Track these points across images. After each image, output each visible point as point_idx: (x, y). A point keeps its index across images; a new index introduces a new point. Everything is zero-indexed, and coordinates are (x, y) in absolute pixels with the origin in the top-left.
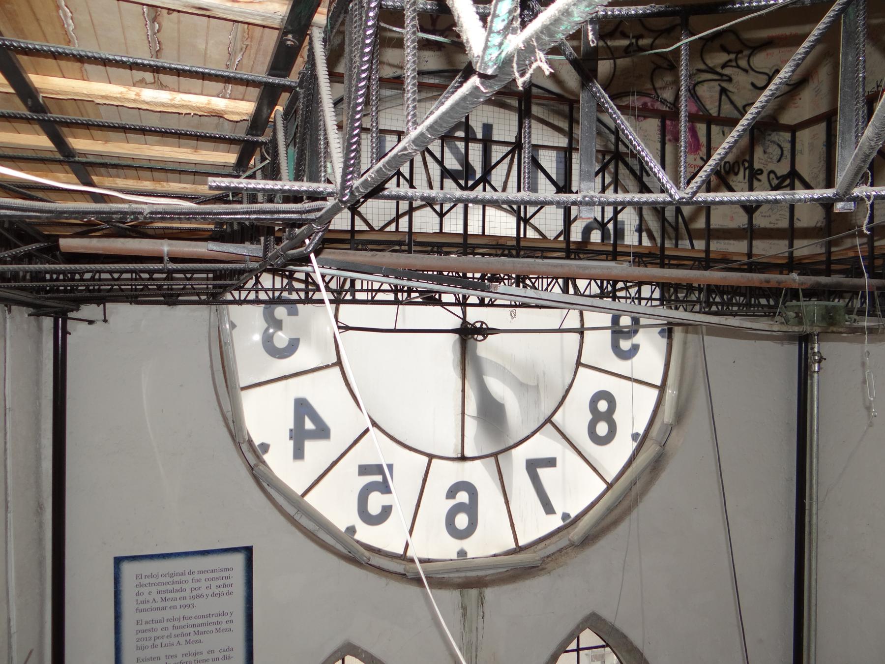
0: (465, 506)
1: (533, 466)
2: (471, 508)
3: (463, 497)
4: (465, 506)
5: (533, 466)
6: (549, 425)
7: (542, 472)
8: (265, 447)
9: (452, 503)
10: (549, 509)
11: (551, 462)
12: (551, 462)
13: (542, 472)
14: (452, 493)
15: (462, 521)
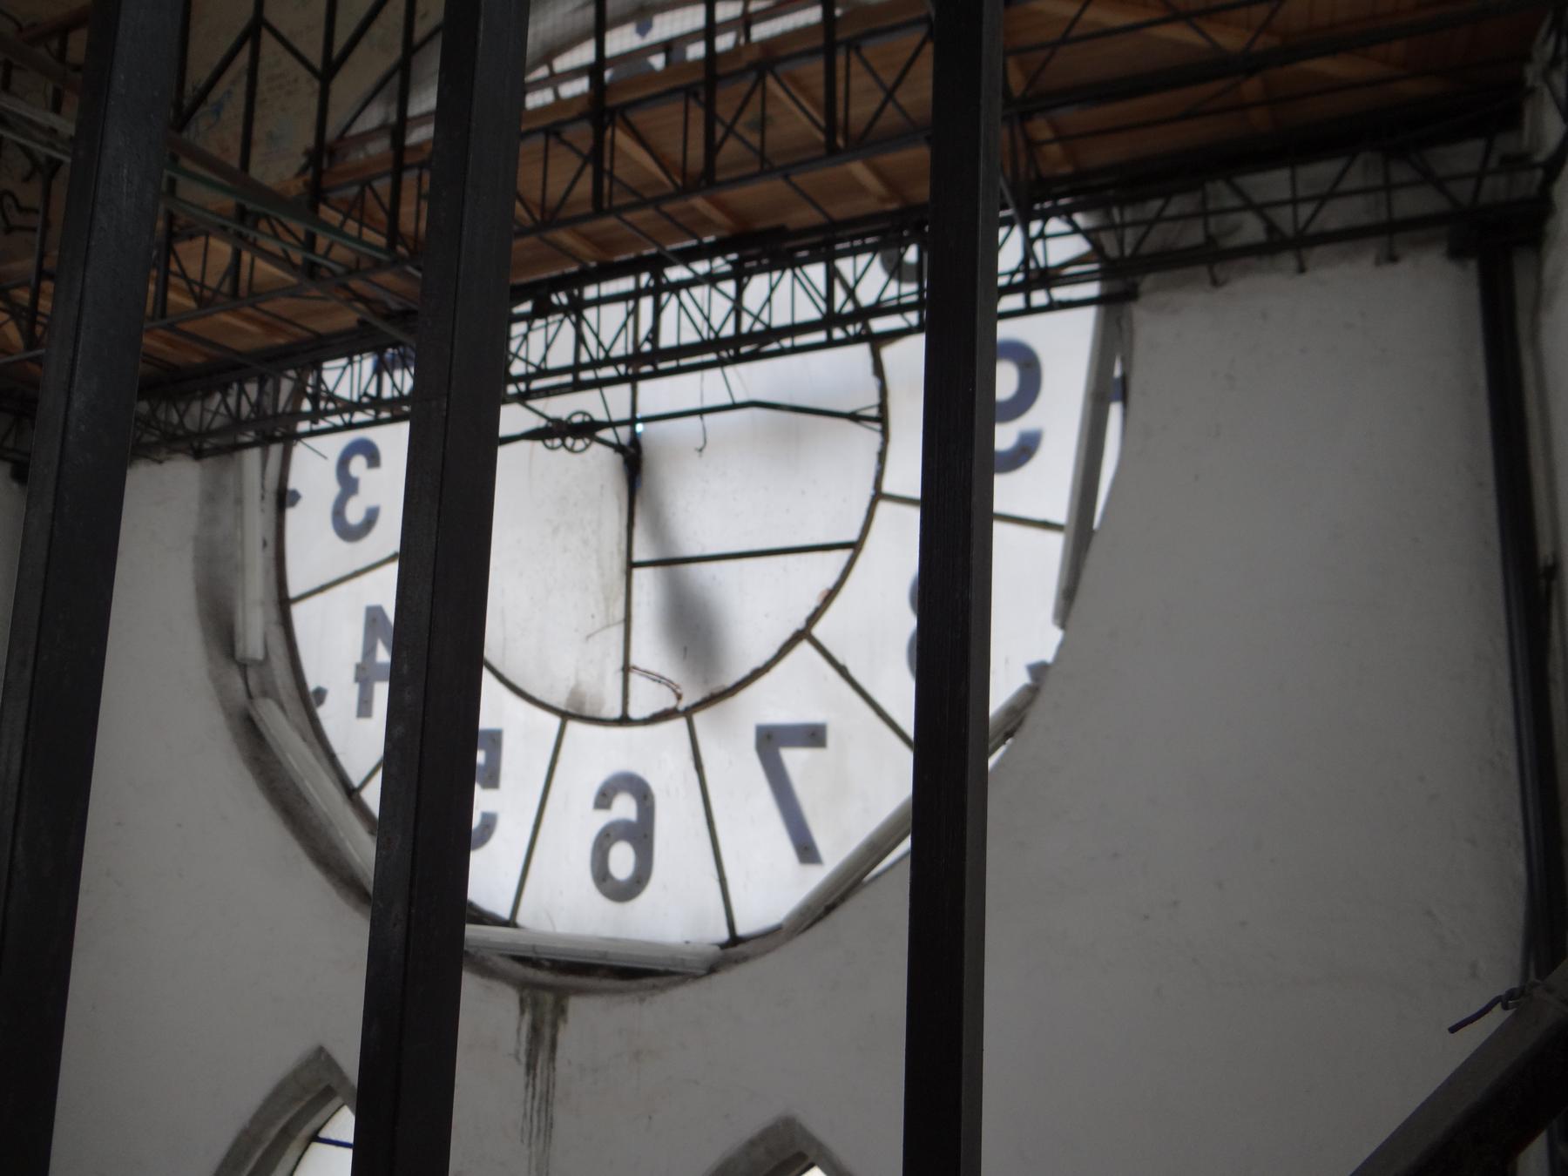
0: (630, 833)
1: (771, 741)
2: (640, 834)
3: (625, 808)
4: (630, 833)
5: (771, 741)
6: (805, 647)
7: (794, 759)
8: (320, 694)
9: (602, 819)
10: (807, 851)
11: (813, 736)
12: (813, 736)
13: (794, 759)
14: (604, 799)
15: (622, 860)
